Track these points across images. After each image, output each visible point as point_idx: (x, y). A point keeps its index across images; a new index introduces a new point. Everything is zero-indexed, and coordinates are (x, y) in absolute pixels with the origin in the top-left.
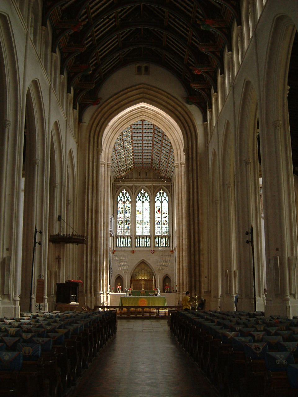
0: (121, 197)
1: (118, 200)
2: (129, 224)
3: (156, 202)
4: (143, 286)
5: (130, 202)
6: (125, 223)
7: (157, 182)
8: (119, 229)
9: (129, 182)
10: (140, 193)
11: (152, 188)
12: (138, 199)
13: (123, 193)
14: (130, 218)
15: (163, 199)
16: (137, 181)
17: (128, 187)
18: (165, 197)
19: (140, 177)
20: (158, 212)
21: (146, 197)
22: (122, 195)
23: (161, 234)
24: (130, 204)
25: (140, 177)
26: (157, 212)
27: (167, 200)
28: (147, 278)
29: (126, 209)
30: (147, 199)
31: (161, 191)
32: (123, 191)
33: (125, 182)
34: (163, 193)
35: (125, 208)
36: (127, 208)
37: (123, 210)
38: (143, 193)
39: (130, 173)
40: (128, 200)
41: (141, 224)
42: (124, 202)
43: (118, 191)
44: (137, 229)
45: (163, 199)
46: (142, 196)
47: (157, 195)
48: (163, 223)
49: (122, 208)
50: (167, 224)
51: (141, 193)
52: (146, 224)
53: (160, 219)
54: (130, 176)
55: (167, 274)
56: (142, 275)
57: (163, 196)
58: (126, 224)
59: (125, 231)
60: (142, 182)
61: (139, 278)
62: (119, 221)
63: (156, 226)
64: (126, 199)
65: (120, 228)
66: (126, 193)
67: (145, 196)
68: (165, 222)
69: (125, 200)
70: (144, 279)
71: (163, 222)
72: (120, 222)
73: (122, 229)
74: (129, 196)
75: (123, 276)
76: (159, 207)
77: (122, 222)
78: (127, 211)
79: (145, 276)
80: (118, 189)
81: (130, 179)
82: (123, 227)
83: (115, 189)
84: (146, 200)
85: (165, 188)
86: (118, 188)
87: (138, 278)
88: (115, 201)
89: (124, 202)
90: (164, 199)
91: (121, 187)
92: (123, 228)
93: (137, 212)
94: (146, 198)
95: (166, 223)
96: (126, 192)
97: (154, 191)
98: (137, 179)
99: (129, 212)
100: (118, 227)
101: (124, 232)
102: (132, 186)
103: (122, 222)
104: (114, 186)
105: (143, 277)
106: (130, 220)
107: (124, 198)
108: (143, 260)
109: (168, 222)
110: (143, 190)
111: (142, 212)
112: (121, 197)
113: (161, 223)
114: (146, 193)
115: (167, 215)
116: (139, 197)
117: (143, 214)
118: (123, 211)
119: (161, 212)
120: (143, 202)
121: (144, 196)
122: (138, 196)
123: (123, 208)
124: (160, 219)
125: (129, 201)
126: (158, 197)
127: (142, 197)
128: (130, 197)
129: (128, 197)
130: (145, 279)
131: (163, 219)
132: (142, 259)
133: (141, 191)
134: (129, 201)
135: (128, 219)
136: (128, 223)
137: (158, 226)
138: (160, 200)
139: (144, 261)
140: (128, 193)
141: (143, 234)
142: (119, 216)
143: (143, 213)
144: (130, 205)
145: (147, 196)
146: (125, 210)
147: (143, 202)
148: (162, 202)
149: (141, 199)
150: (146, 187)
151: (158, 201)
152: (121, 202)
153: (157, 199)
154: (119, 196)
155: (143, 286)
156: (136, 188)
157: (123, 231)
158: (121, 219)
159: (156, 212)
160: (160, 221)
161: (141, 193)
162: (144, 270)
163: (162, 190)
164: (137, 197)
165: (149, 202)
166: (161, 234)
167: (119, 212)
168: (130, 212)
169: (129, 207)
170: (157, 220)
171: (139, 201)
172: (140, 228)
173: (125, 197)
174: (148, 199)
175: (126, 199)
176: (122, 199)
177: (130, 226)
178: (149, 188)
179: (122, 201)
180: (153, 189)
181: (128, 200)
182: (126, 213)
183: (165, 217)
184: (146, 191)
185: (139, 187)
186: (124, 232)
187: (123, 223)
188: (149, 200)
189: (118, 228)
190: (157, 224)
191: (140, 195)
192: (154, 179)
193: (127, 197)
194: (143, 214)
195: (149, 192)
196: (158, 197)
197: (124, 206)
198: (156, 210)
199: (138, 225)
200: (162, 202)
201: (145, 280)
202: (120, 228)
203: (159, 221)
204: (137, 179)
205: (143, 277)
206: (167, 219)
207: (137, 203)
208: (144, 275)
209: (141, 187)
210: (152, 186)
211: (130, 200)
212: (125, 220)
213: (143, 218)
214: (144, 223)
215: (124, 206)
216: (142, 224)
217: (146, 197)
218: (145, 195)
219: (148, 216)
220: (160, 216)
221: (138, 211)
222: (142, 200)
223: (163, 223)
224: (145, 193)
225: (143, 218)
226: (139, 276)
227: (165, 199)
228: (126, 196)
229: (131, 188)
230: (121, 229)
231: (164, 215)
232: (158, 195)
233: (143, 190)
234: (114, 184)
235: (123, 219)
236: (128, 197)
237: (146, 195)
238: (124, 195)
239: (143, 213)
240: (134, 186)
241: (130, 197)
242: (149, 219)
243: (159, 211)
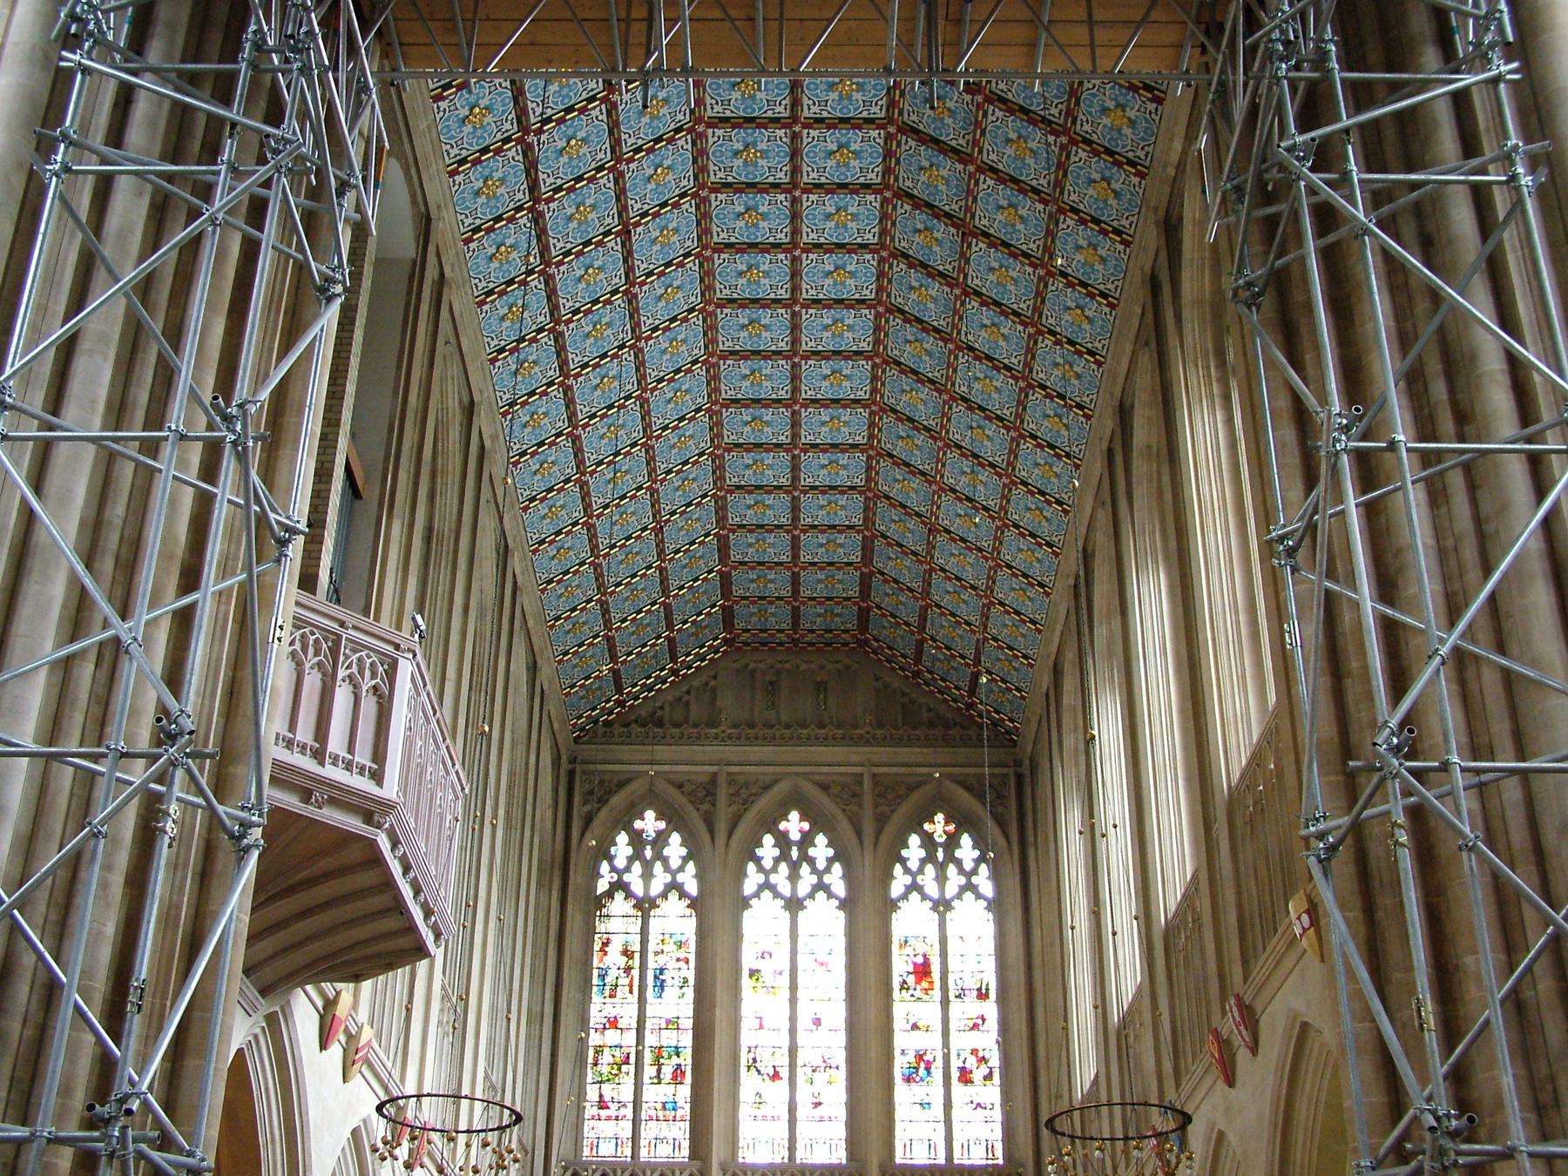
0: (620, 863)
1: (602, 886)
2: (678, 1075)
3: (892, 905)
5: (694, 904)
6: (649, 1071)
7: (905, 753)
8: (595, 1111)
9: (683, 751)
10: (768, 840)
11: (868, 800)
12: (752, 880)
13: (637, 840)
14: (688, 1024)
15: (955, 880)
16: (751, 741)
17: (680, 786)
18: (968, 865)
19: (771, 715)
20: (911, 980)
21: (821, 865)
22: (629, 851)
23: (941, 1160)
24: (694, 919)
25: (771, 715)
26: (904, 986)
27: (987, 887)
29: (662, 959)
30: (827, 879)
31: (938, 827)
32: (638, 824)
33: (662, 751)
34: (952, 842)
35: (652, 946)
36: (670, 947)
37: (636, 962)
38: (795, 836)
39: (695, 683)
40: (674, 886)
41: (776, 1076)
42: (645, 906)
43: (603, 815)
44: (744, 1112)
45: (955, 880)
46: (784, 856)
47: (904, 853)
48: (955, 1074)
49: (627, 953)
50: (989, 1077)
51: (783, 841)
52: (820, 1077)
53: (931, 1042)
54: (695, 712)
57: (951, 858)
58: (658, 1078)
59: (649, 1131)
60: (787, 752)
62: (599, 1050)
63: (902, 1093)
64: (660, 879)
65: (602, 1104)
66: (661, 839)
67: (811, 862)
68: (971, 1063)
69: (656, 887)
71: (955, 1064)
72: (606, 1058)
73: (623, 1111)
74: (685, 860)
76: (921, 949)
77: (626, 1062)
78: (666, 976)
80: (603, 801)
81: (696, 726)
82: (627, 1094)
83: (577, 798)
84: (821, 886)
85: (962, 795)
86: (602, 792)
88: (570, 893)
89: (645, 906)
90: (963, 880)
91: (621, 785)
92: (629, 1112)
93: (746, 982)
94: (820, 874)
95: (978, 1074)
96: (662, 825)
97: (881, 821)
98: (748, 731)
99: (686, 980)
100: (592, 1093)
101: (635, 1138)
102: (714, 778)
103: (626, 1062)
104: (571, 774)
106: (687, 1040)
107: (647, 876)
109: (995, 1061)
110: (794, 815)
111: (785, 981)
112: (620, 863)
113: (938, 1066)
114: (821, 839)
115: (990, 1009)
116: (767, 863)
117: (793, 1001)
118: (635, 973)
119: (937, 985)
120: (794, 905)
121: (805, 858)
122: (758, 860)
123: (637, 947)
124: (931, 1042)
125: (683, 894)
126: (913, 865)
127: (783, 868)
128: (691, 864)
129: (675, 863)
131: (956, 1041)
133: (783, 826)
134: (683, 894)
135: (669, 1038)
136: (667, 1071)
137: (918, 1091)
138: (932, 889)
140: (675, 838)
141: (792, 1148)
142: (599, 1009)
143: (793, 987)
144: (687, 927)
145: (830, 861)
146: (652, 963)
147: (794, 905)
148: (942, 906)
149: (781, 878)
150: (824, 787)
151: (915, 896)
152: (619, 905)
153: (908, 880)
154: (610, 859)
156: (745, 793)
157: (625, 1129)
158: (612, 1037)
159: (896, 985)
160: (928, 1057)
161: (783, 841)
163: (940, 817)
164: (751, 867)
165: (844, 905)
166: (941, 1160)
167: (602, 977)
168: (692, 982)
169: (680, 945)
170: (905, 1043)
171: (767, 894)
172: (766, 1110)
173: (658, 867)
174: (836, 879)
175: (660, 879)
176: (634, 879)
177: (685, 1091)
178: (847, 793)
179: (629, 894)
180: (876, 806)
181: (674, 886)
182: (661, 986)
183: (975, 1027)
184: (818, 821)
185: (767, 788)
186: (635, 1138)
187: (632, 1068)
188: (839, 888)
189: (591, 1110)
190: (908, 1079)
191: (768, 849)
192: (880, 725)
193: (667, 868)
194: (793, 1001)
195: (845, 826)
196: (913, 865)
197: (644, 933)
198: (901, 966)
199: (749, 1084)
200: (942, 906)
202: (602, 1104)
203: (919, 1057)
204: (752, 726)
206: (988, 1041)
207: (746, 914)
209: (783, 787)
210: (867, 781)
211: (692, 887)
212: (650, 1040)
213: (793, 1031)
214: (800, 1071)
215: (644, 933)
216: (784, 1073)
217: (821, 865)
218: (812, 852)
219: (836, 1014)
220: (929, 1012)
221: (752, 973)
222: (785, 888)
223: (955, 1074)
224: (807, 840)
225: (793, 1031)
227: (970, 887)
228: (665, 861)
229: (704, 793)
230: (612, 1112)
231: (963, 1011)
232: (914, 850)
233: (794, 815)
234: (573, 761)
235: (630, 1039)
236: (675, 863)
237: (821, 849)
238: (648, 853)
239: (793, 987)
240: (722, 780)
241: (691, 864)
242: (841, 1039)
243: (922, 971)
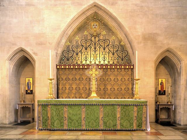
4: (94, 85)
28: (106, 62)
55: (168, 51)
56: (93, 53)
61: (84, 62)
70: (97, 63)
75: (34, 56)
79: (102, 56)
87: (79, 63)
105: (95, 57)
108: (95, 6)
130: (102, 63)
132: (91, 2)
139: (100, 13)
155: (94, 85)
162: (97, 39)
201: (100, 67)
205: (95, 57)
208: (97, 52)
226: (84, 57)
